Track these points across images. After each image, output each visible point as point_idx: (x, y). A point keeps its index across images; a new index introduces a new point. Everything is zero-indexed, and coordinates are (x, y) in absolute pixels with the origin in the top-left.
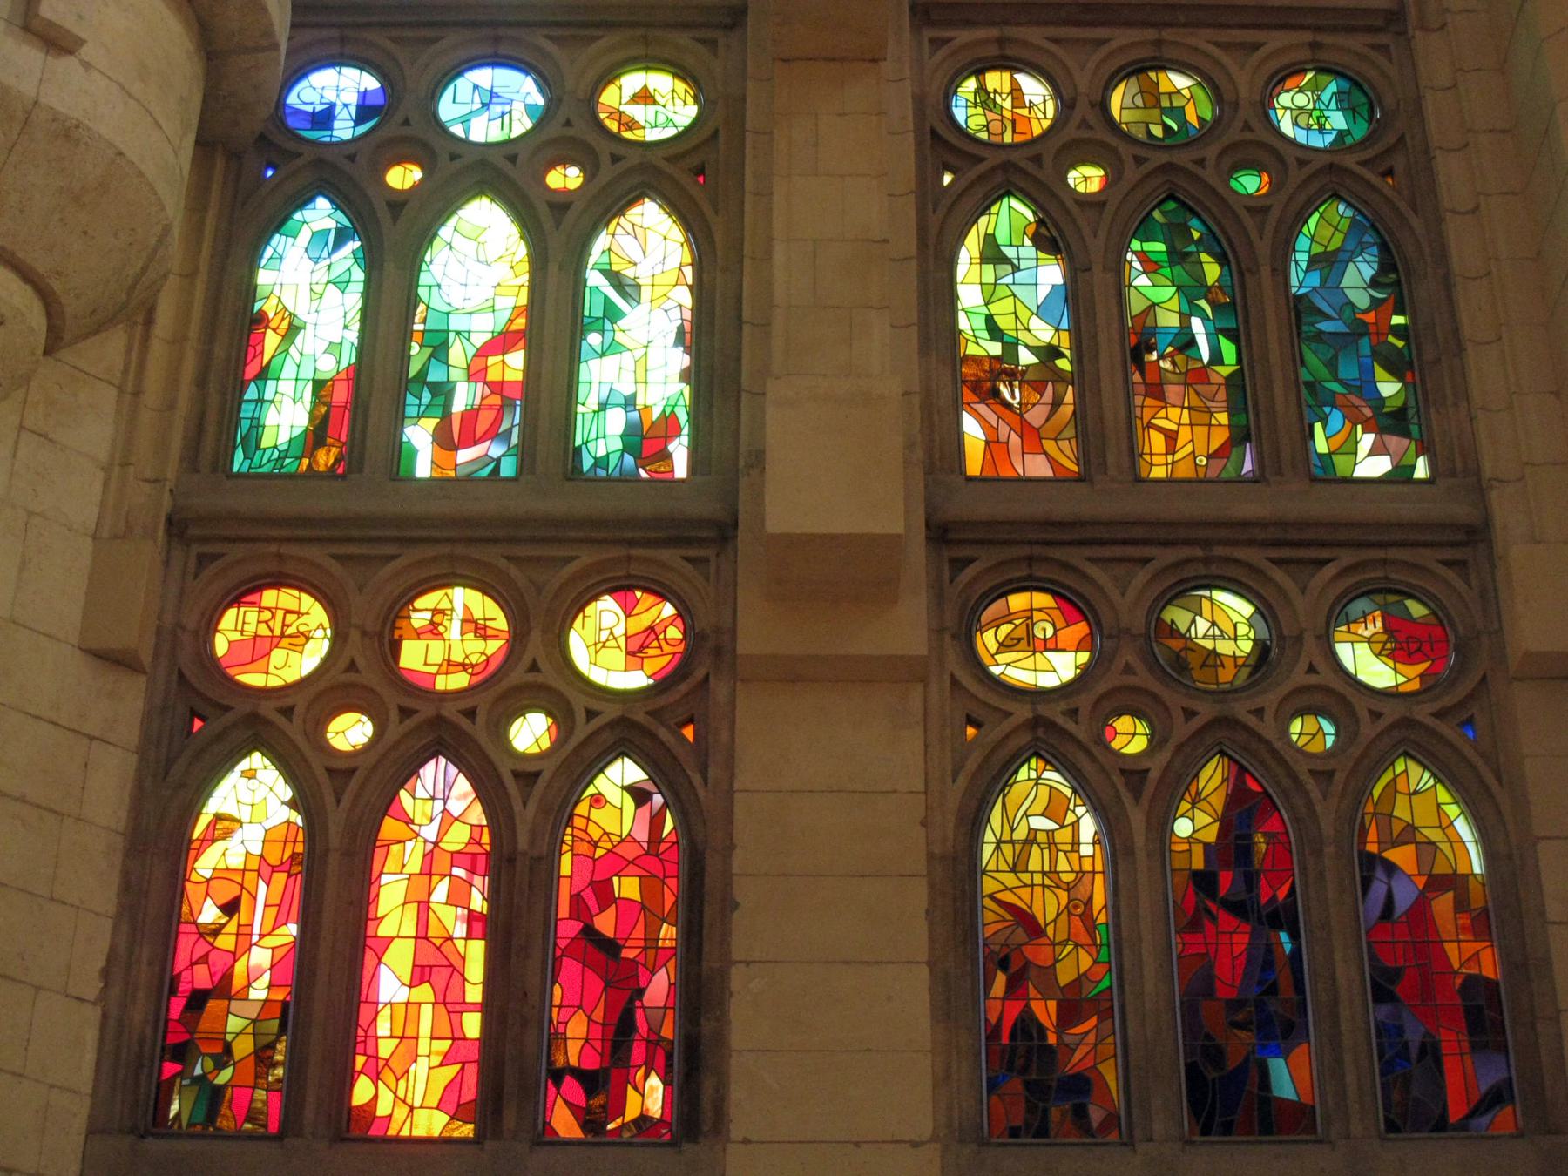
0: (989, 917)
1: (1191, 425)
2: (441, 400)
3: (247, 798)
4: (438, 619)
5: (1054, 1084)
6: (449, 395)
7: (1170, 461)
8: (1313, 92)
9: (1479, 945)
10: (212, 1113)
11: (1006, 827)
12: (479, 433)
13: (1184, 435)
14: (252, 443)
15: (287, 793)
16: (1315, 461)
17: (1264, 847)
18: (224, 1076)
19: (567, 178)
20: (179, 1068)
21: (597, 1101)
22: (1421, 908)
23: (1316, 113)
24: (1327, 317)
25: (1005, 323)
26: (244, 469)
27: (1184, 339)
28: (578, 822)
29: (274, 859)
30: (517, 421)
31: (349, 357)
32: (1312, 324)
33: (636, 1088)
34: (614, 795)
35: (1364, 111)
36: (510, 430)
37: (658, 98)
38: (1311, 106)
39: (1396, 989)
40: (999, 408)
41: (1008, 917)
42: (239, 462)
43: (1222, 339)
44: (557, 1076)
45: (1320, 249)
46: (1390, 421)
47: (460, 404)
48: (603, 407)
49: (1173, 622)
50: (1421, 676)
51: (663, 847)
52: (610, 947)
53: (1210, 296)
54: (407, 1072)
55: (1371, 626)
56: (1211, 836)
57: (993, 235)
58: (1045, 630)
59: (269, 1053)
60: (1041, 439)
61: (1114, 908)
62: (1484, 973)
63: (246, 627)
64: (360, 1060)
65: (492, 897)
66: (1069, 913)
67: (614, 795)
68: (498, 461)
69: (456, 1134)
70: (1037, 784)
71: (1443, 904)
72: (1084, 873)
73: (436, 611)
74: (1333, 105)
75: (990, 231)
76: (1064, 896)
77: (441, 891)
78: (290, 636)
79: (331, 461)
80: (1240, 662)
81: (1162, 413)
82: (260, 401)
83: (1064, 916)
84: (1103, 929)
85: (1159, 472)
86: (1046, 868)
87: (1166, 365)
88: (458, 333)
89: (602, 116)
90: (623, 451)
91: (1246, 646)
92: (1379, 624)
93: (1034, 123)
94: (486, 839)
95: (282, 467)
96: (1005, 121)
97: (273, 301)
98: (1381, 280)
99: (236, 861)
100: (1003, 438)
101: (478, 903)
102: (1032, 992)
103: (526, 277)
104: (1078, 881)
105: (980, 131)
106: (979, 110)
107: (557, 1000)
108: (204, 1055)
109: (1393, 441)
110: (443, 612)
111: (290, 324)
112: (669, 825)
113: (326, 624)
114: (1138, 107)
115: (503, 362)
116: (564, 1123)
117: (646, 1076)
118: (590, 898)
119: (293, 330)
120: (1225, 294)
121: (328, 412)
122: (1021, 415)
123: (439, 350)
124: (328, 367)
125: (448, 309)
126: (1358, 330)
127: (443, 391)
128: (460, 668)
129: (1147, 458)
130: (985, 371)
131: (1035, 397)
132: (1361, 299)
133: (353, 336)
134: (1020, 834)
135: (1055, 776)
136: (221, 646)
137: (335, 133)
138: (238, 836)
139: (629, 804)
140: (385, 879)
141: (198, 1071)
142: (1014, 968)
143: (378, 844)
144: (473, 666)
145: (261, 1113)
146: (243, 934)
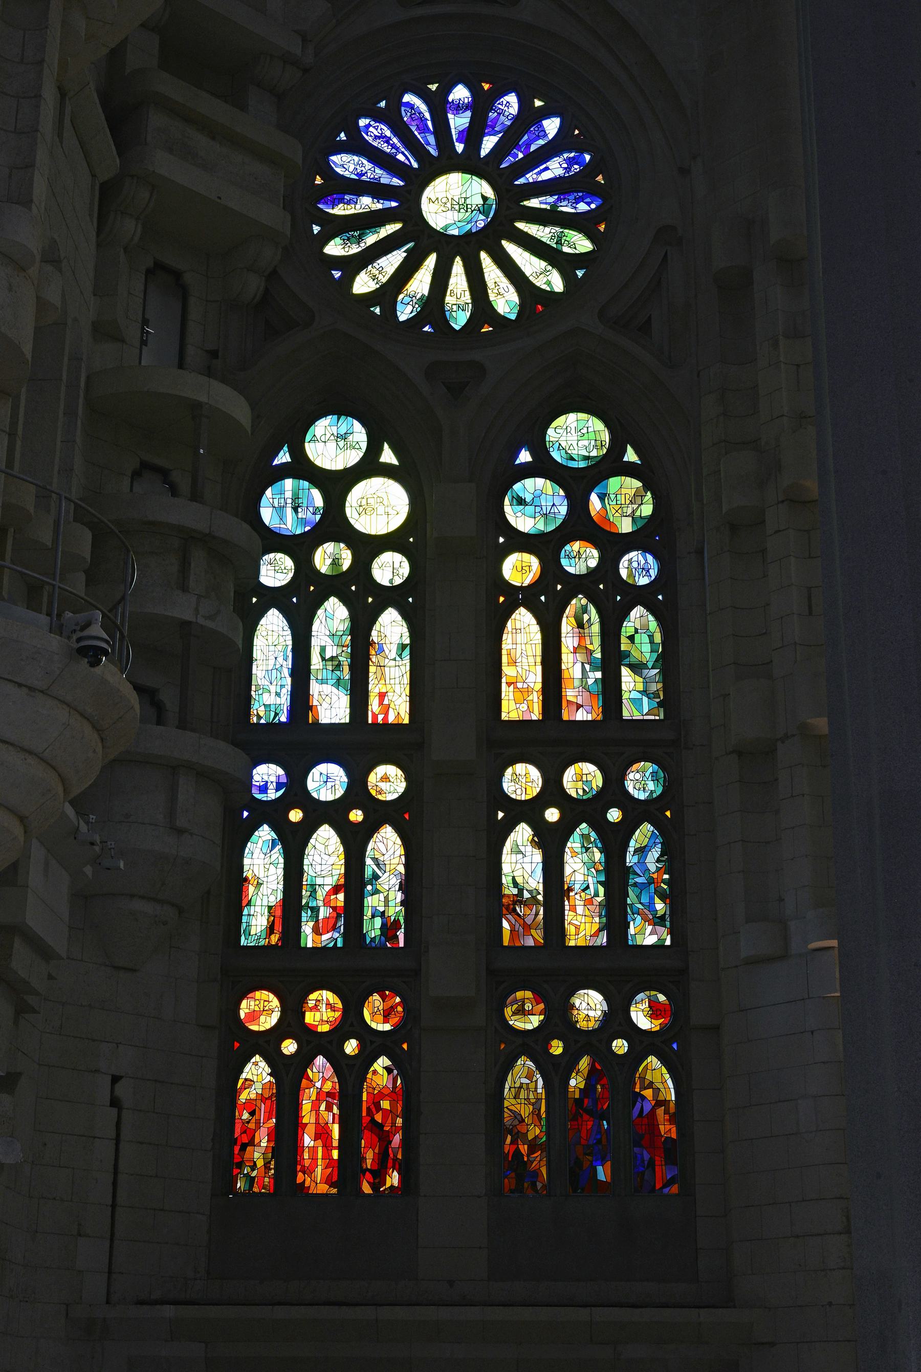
3: (255, 1072)
8: (643, 772)
10: (251, 1186)
11: (513, 1082)
16: (630, 938)
17: (600, 1089)
18: (254, 1174)
19: (356, 816)
22: (653, 1111)
23: (643, 782)
24: (641, 876)
25: (519, 880)
27: (585, 886)
30: (342, 923)
31: (280, 896)
33: (390, 1176)
34: (380, 1070)
35: (661, 781)
37: (391, 779)
38: (641, 779)
41: (513, 1115)
42: (243, 942)
43: (600, 886)
45: (639, 846)
48: (373, 916)
49: (574, 1003)
50: (660, 1024)
51: (397, 1090)
52: (381, 1126)
53: (596, 867)
54: (315, 1171)
55: (644, 1004)
56: (582, 1086)
59: (268, 1165)
60: (530, 929)
61: (547, 1111)
62: (672, 1137)
63: (251, 1007)
64: (299, 1167)
66: (533, 1114)
67: (380, 1070)
68: (336, 939)
70: (524, 1066)
71: (660, 1111)
72: (538, 1099)
73: (317, 1001)
74: (650, 779)
75: (515, 839)
76: (531, 1107)
77: (323, 1107)
78: (266, 1010)
79: (277, 940)
81: (575, 918)
82: (249, 915)
83: (531, 1116)
84: (544, 1119)
85: (572, 943)
86: (526, 1098)
88: (319, 885)
89: (370, 788)
90: (381, 935)
91: (599, 1013)
92: (647, 1004)
94: (337, 1087)
95: (259, 943)
96: (523, 789)
97: (251, 872)
99: (253, 1096)
101: (335, 1110)
102: (520, 1142)
103: (343, 861)
104: (536, 1102)
107: (363, 1146)
108: (247, 1166)
110: (319, 1001)
111: (258, 882)
112: (399, 1082)
113: (279, 1006)
115: (336, 897)
116: (367, 1189)
117: (393, 1172)
118: (373, 1107)
119: (259, 885)
121: (274, 919)
122: (523, 919)
123: (313, 892)
125: (315, 875)
126: (651, 881)
127: (315, 910)
128: (326, 1023)
129: (568, 936)
130: (511, 901)
131: (528, 912)
132: (652, 867)
133: (281, 887)
134: (517, 1085)
135: (531, 1063)
136: (242, 1016)
137: (268, 795)
138: (253, 1087)
139: (386, 1074)
140: (304, 1102)
141: (245, 1172)
143: (301, 1089)
144: (331, 1022)
145: (267, 1186)
146: (258, 1122)
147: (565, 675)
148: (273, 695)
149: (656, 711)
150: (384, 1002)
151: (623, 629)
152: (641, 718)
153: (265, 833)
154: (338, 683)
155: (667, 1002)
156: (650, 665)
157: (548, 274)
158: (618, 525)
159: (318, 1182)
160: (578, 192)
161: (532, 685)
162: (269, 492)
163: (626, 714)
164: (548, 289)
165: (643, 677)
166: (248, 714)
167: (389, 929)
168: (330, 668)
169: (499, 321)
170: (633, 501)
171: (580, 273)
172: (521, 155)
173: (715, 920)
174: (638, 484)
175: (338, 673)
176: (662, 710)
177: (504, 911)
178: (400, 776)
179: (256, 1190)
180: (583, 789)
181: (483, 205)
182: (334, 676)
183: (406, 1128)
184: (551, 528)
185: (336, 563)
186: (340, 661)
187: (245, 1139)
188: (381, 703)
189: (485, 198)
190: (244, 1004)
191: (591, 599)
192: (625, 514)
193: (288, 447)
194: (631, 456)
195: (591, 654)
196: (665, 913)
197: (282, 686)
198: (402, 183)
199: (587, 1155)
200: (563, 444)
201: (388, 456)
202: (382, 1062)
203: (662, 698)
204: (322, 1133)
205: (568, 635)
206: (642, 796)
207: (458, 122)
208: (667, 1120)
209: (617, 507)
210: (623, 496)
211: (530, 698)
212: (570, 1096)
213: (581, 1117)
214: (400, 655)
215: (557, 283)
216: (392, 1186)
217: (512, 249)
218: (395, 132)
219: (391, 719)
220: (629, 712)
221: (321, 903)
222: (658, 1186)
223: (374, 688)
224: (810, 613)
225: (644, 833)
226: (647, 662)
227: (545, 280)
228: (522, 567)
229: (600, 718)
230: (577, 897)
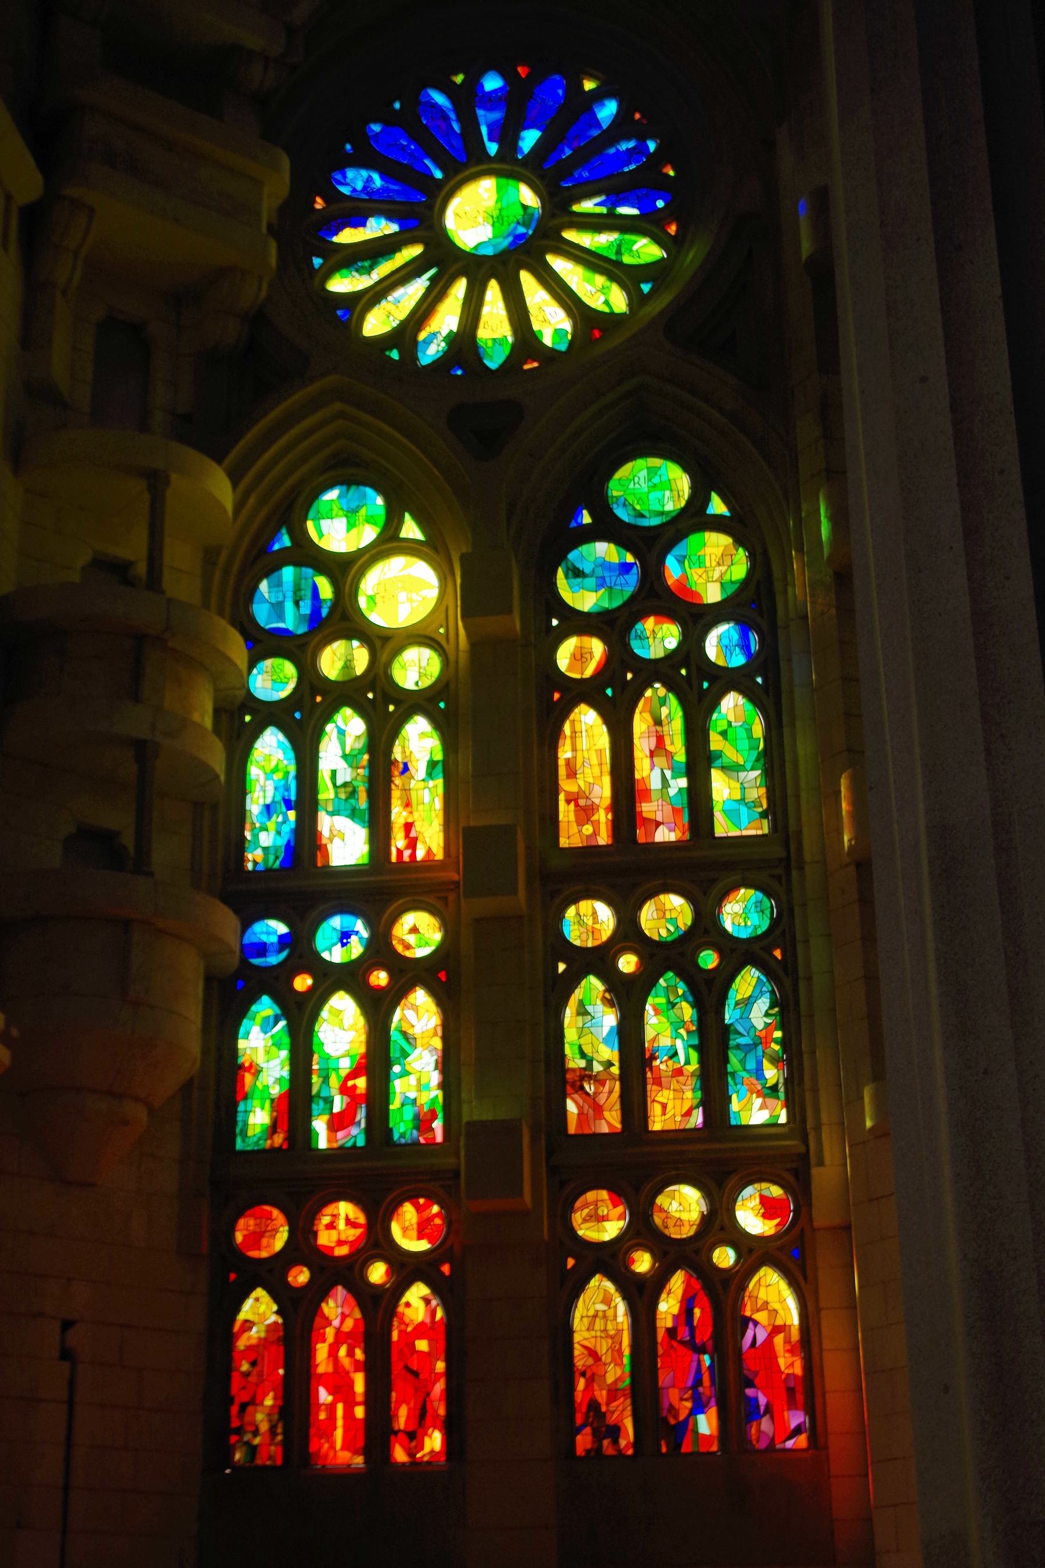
0: (576, 1353)
1: (674, 1099)
2: (328, 1105)
5: (604, 1429)
6: (332, 1102)
7: (663, 1120)
9: (795, 1358)
11: (585, 1311)
13: (669, 1107)
14: (244, 1134)
15: (275, 1308)
18: (257, 1441)
21: (413, 1444)
23: (743, 916)
24: (742, 1035)
25: (587, 1050)
27: (672, 1052)
31: (286, 1086)
32: (735, 1039)
35: (768, 912)
38: (741, 912)
40: (584, 1095)
42: (239, 1145)
44: (396, 1433)
46: (769, 1091)
47: (337, 1107)
50: (777, 1225)
52: (416, 1374)
53: (685, 1027)
56: (675, 1310)
57: (582, 1000)
58: (603, 1211)
66: (612, 1350)
68: (355, 1137)
70: (599, 1288)
71: (779, 1340)
74: (753, 910)
75: (581, 998)
77: (343, 1351)
80: (691, 1223)
81: (660, 1093)
83: (610, 1351)
87: (663, 1067)
88: (334, 1069)
93: (603, 932)
97: (247, 1057)
99: (254, 1341)
100: (585, 1112)
101: (359, 1354)
102: (596, 1387)
105: (576, 939)
106: (576, 927)
109: (770, 1101)
114: (654, 919)
120: (693, 1025)
122: (594, 1099)
123: (326, 1079)
124: (276, 1091)
127: (329, 1101)
134: (591, 1313)
142: (588, 1375)
146: (260, 1374)
148: (272, 833)
149: (757, 824)
153: (265, 1007)
154: (353, 814)
156: (748, 766)
157: (605, 291)
161: (597, 801)
162: (264, 586)
163: (719, 831)
164: (606, 310)
165: (740, 781)
166: (241, 859)
167: (423, 1122)
168: (343, 796)
169: (549, 356)
170: (721, 562)
172: (568, 152)
175: (353, 801)
176: (765, 822)
177: (569, 1089)
178: (432, 926)
179: (259, 1462)
180: (668, 930)
181: (523, 216)
182: (348, 806)
183: (449, 1373)
185: (348, 666)
187: (245, 1397)
189: (525, 207)
190: (242, 1222)
191: (670, 687)
192: (710, 579)
195: (672, 757)
197: (284, 822)
199: (687, 1400)
200: (630, 499)
201: (411, 530)
203: (765, 806)
204: (341, 1387)
206: (744, 934)
209: (700, 571)
211: (595, 818)
215: (618, 301)
216: (432, 1451)
217: (558, 264)
220: (723, 827)
221: (337, 1091)
223: (398, 815)
226: (744, 762)
227: (602, 299)
228: (582, 655)
229: (687, 836)
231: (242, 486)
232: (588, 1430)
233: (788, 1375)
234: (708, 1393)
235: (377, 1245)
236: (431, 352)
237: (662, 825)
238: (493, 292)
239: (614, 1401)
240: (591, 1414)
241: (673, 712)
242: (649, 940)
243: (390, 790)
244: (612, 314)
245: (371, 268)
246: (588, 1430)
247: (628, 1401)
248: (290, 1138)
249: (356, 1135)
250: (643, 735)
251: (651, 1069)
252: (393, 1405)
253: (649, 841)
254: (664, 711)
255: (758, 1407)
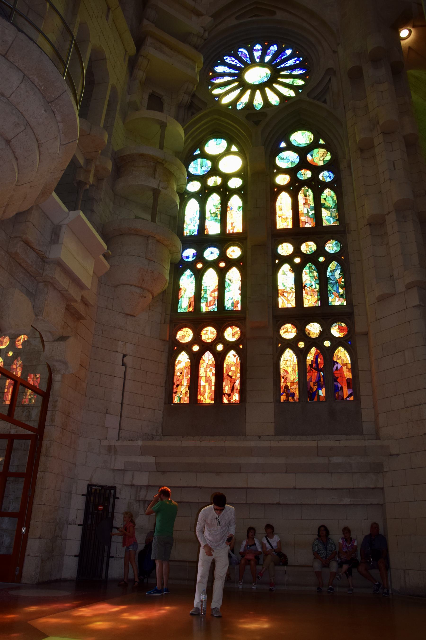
2: (206, 300)
4: (207, 332)
6: (207, 299)
12: (212, 304)
16: (329, 303)
19: (222, 265)
20: (175, 395)
21: (230, 398)
23: (332, 247)
24: (333, 280)
26: (180, 312)
27: (311, 285)
28: (226, 360)
29: (186, 367)
30: (217, 302)
31: (193, 294)
35: (339, 246)
36: (216, 304)
39: (338, 380)
41: (284, 371)
42: (179, 311)
43: (316, 284)
44: (224, 394)
45: (332, 269)
46: (341, 296)
48: (229, 300)
51: (238, 363)
52: (231, 377)
55: (336, 327)
56: (312, 359)
64: (199, 393)
65: (215, 370)
69: (211, 403)
71: (344, 368)
74: (335, 246)
76: (292, 368)
77: (209, 370)
80: (317, 334)
81: (307, 297)
83: (292, 371)
94: (214, 362)
98: (341, 274)
101: (214, 371)
102: (287, 382)
104: (294, 366)
109: (341, 299)
110: (207, 331)
119: (185, 290)
123: (206, 292)
126: (337, 282)
127: (206, 298)
131: (289, 295)
132: (337, 277)
134: (286, 360)
137: (190, 259)
140: (201, 369)
141: (178, 395)
142: (285, 378)
146: (183, 377)
147: (300, 213)
149: (336, 223)
150: (233, 330)
151: (322, 196)
152: (330, 225)
153: (188, 272)
155: (346, 326)
156: (333, 207)
158: (318, 163)
159: (206, 399)
160: (299, 68)
161: (288, 217)
164: (289, 96)
167: (234, 304)
168: (213, 216)
170: (323, 155)
171: (300, 91)
172: (278, 60)
173: (364, 292)
174: (325, 150)
175: (216, 217)
176: (338, 222)
177: (279, 295)
180: (309, 251)
182: (215, 219)
183: (241, 377)
184: (293, 166)
185: (215, 182)
186: (216, 214)
187: (178, 383)
188: (232, 226)
189: (267, 74)
193: (199, 149)
194: (321, 142)
196: (343, 294)
197: (196, 223)
198: (238, 72)
199: (316, 386)
200: (297, 141)
201: (234, 148)
202: (232, 353)
203: (338, 218)
204: (208, 380)
205: (301, 199)
206: (332, 252)
207: (257, 54)
208: (348, 371)
210: (319, 154)
212: (307, 363)
213: (312, 371)
214: (239, 210)
216: (236, 400)
218: (236, 59)
219: (235, 231)
220: (325, 223)
221: (209, 296)
222: (345, 397)
224: (395, 169)
225: (333, 265)
229: (314, 226)
230: (308, 289)
231: (187, 136)
232: (285, 394)
233: (348, 378)
234: (322, 383)
235: (220, 339)
236: (240, 106)
237: (307, 223)
238: (258, 93)
239: (293, 386)
240: (286, 389)
241: (310, 193)
242: (304, 253)
243: (227, 214)
244: (291, 97)
245: (224, 88)
246: (285, 394)
247: (297, 386)
248: (195, 308)
249: (214, 308)
250: (301, 199)
251: (305, 290)
252: (224, 386)
253: (303, 227)
254: (307, 193)
255: (338, 388)
